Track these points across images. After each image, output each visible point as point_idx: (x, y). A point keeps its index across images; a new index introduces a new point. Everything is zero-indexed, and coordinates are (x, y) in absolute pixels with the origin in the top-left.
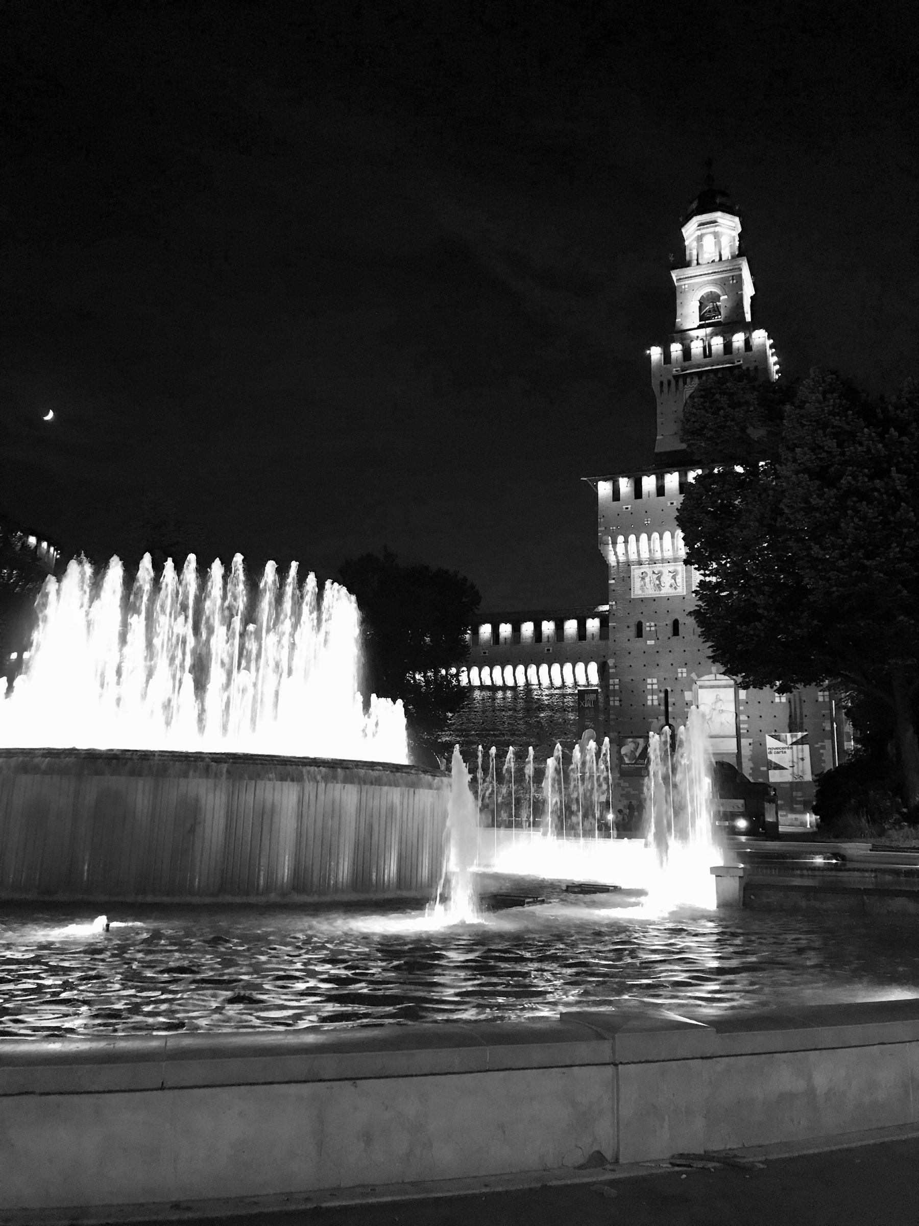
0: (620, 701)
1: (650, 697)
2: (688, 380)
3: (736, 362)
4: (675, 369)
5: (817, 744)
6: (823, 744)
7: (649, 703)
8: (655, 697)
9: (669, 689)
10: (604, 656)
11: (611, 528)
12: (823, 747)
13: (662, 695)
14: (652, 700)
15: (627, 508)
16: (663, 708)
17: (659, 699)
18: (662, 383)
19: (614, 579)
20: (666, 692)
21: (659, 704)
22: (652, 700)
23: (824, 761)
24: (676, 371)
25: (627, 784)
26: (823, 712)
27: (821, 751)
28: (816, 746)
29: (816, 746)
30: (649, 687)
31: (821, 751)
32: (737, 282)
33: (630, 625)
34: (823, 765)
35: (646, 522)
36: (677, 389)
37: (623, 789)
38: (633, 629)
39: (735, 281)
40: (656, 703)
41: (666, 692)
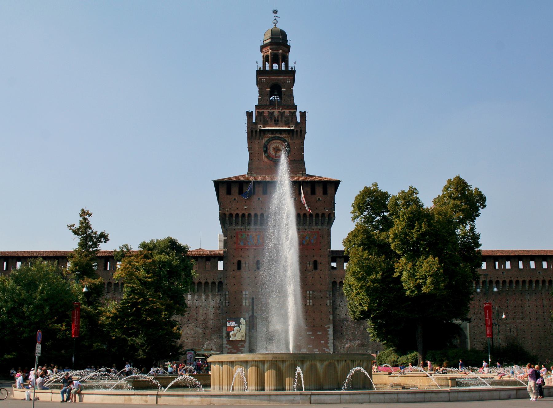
0: (229, 303)
1: (244, 301)
2: (266, 133)
3: (291, 126)
4: (259, 126)
5: (326, 326)
6: (328, 326)
7: (244, 304)
8: (247, 301)
9: (255, 298)
10: (220, 279)
11: (226, 209)
12: (329, 328)
13: (251, 301)
14: (246, 303)
15: (235, 199)
16: (251, 307)
17: (249, 303)
18: (252, 131)
19: (226, 237)
20: (253, 299)
21: (249, 305)
22: (246, 303)
23: (329, 334)
24: (260, 126)
25: (231, 347)
26: (329, 310)
27: (328, 329)
28: (326, 327)
29: (326, 327)
30: (244, 296)
31: (328, 329)
32: (291, 82)
33: (235, 262)
34: (328, 336)
35: (245, 208)
36: (260, 136)
37: (229, 349)
38: (236, 265)
39: (289, 82)
40: (247, 304)
41: (253, 299)
